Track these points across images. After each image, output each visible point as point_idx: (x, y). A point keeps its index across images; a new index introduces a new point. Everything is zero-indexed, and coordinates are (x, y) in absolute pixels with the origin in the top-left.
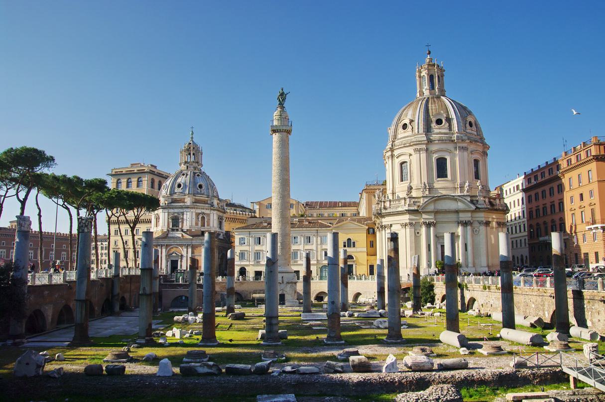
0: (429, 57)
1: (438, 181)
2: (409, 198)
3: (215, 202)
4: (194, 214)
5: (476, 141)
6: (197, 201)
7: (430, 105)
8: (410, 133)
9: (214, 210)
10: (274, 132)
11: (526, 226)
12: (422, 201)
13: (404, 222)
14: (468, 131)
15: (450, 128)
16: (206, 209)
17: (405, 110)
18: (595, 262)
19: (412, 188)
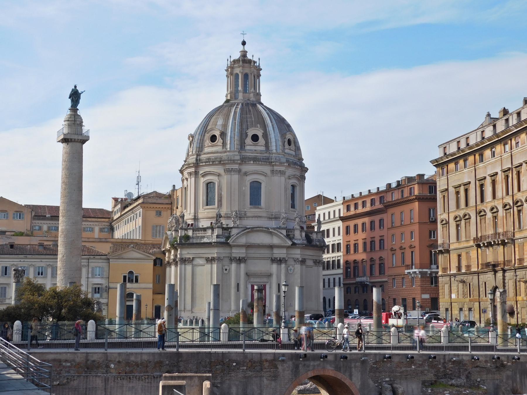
1: (251, 208)
8: (219, 149)
13: (210, 256)
14: (287, 151)
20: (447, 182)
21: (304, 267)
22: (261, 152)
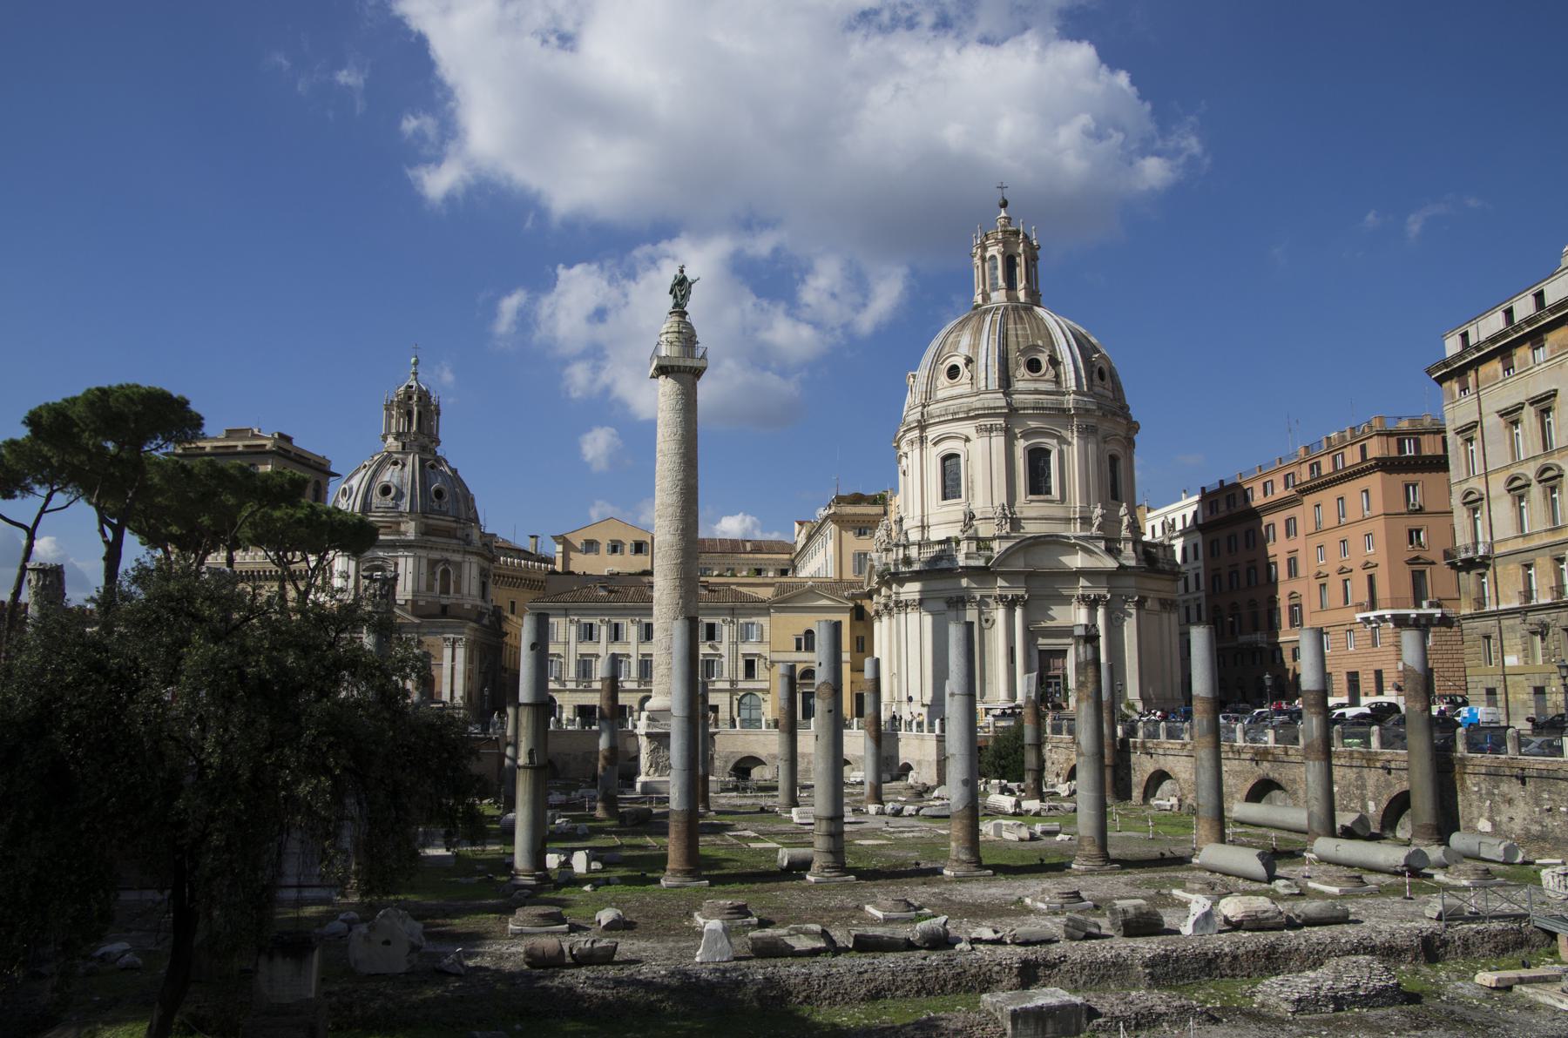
0: (1003, 214)
1: (1031, 501)
2: (968, 538)
3: (475, 535)
4: (424, 563)
5: (1115, 414)
6: (426, 531)
7: (1011, 326)
9: (472, 553)
10: (663, 373)
11: (1203, 607)
12: (998, 547)
15: (1057, 379)
16: (454, 551)
17: (951, 332)
18: (1374, 693)
19: (974, 516)
20: (1477, 407)
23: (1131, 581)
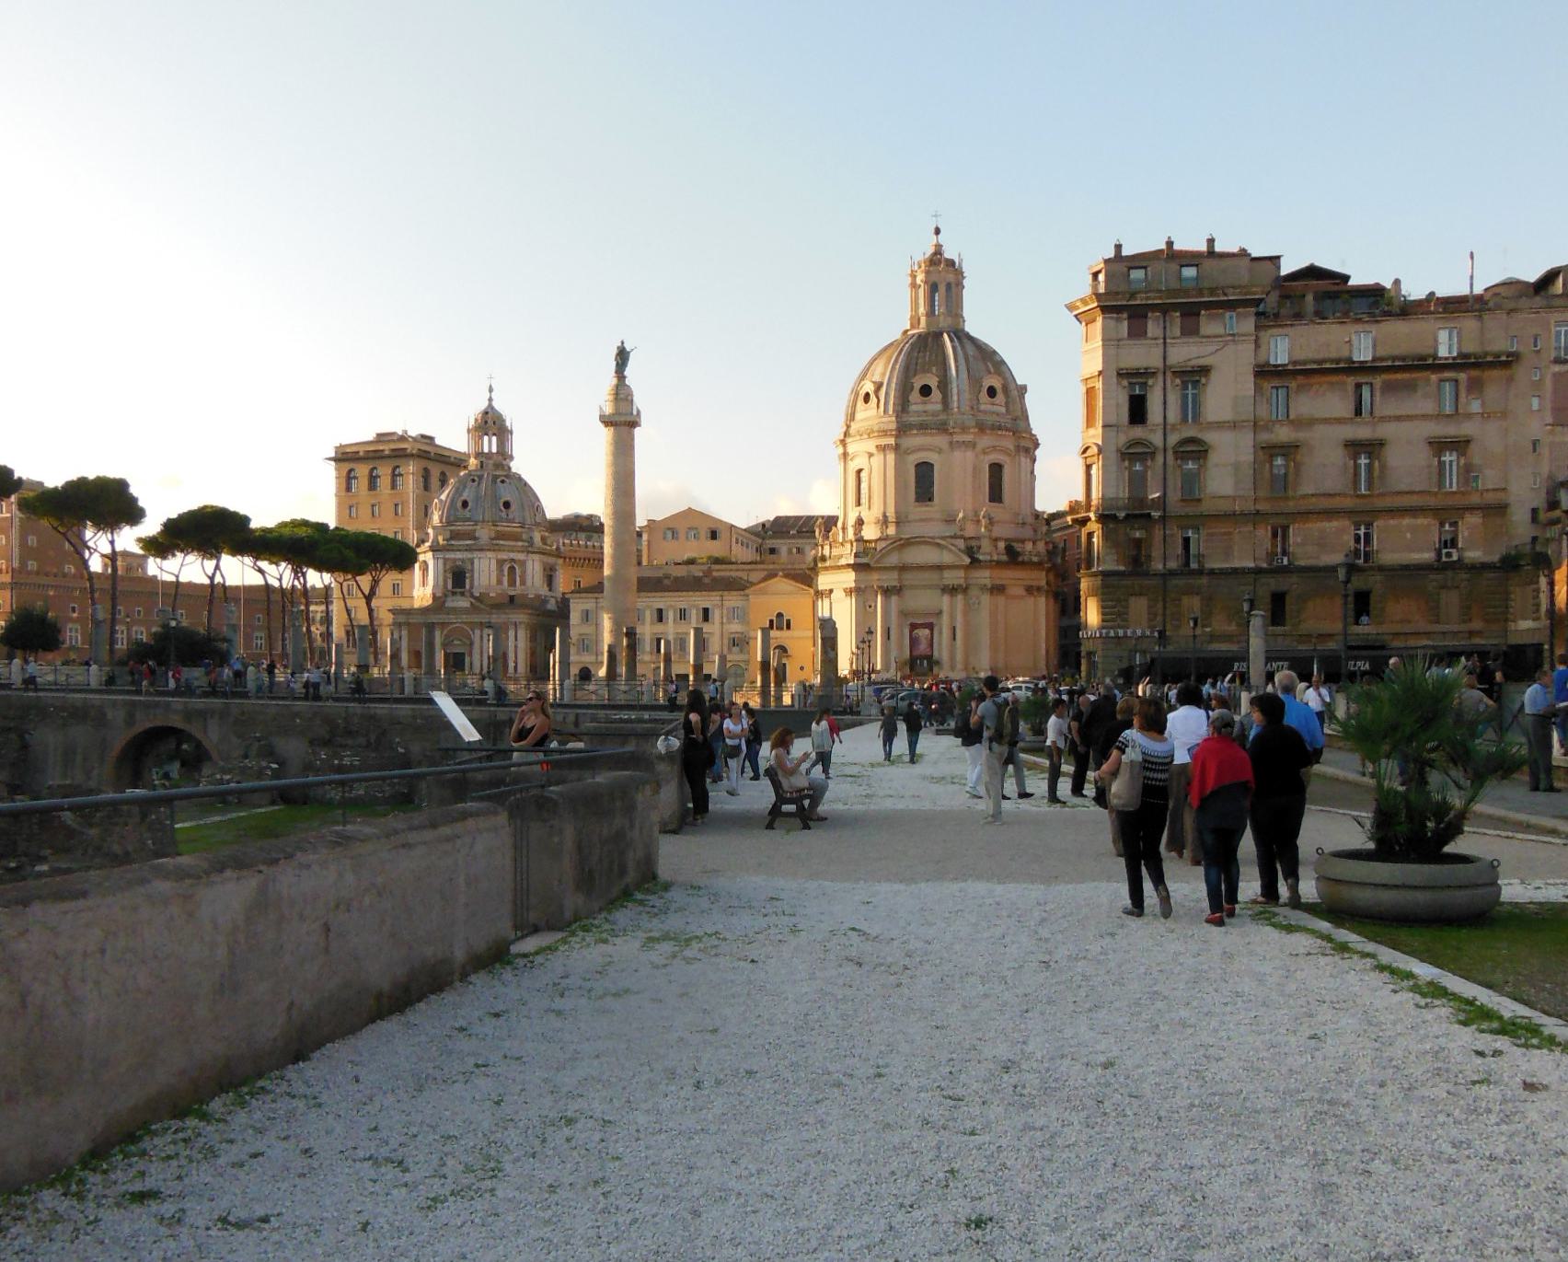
1: (916, 507)
4: (494, 563)
5: (997, 428)
14: (983, 407)
21: (1001, 600)
22: (935, 414)
23: (987, 573)
